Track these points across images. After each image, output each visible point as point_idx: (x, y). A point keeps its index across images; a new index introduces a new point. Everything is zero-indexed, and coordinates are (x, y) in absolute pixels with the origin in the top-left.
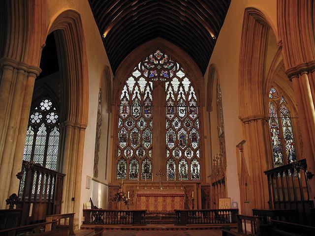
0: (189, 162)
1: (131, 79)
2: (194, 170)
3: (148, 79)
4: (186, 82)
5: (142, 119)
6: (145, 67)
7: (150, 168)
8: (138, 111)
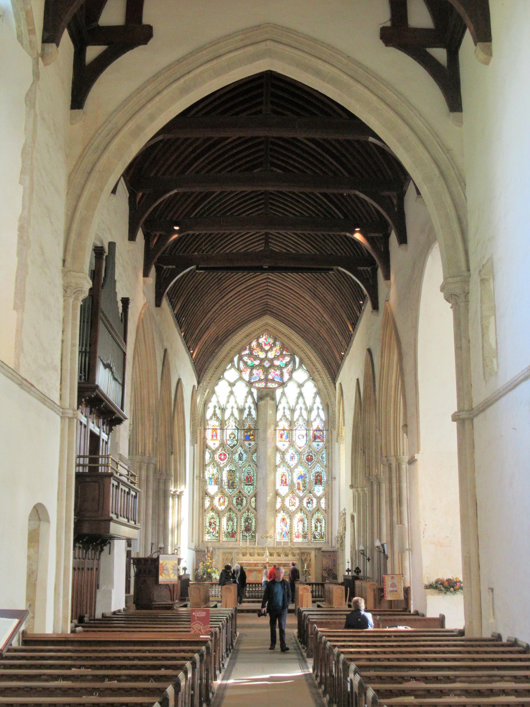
2: (316, 527)
3: (250, 384)
4: (310, 389)
5: (240, 450)
6: (245, 363)
7: (253, 524)
8: (234, 438)
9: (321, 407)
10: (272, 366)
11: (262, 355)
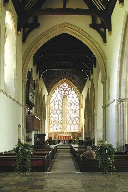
0: (75, 125)
1: (54, 94)
3: (61, 95)
4: (75, 96)
6: (60, 90)
9: (78, 100)
10: (66, 90)
11: (64, 88)
